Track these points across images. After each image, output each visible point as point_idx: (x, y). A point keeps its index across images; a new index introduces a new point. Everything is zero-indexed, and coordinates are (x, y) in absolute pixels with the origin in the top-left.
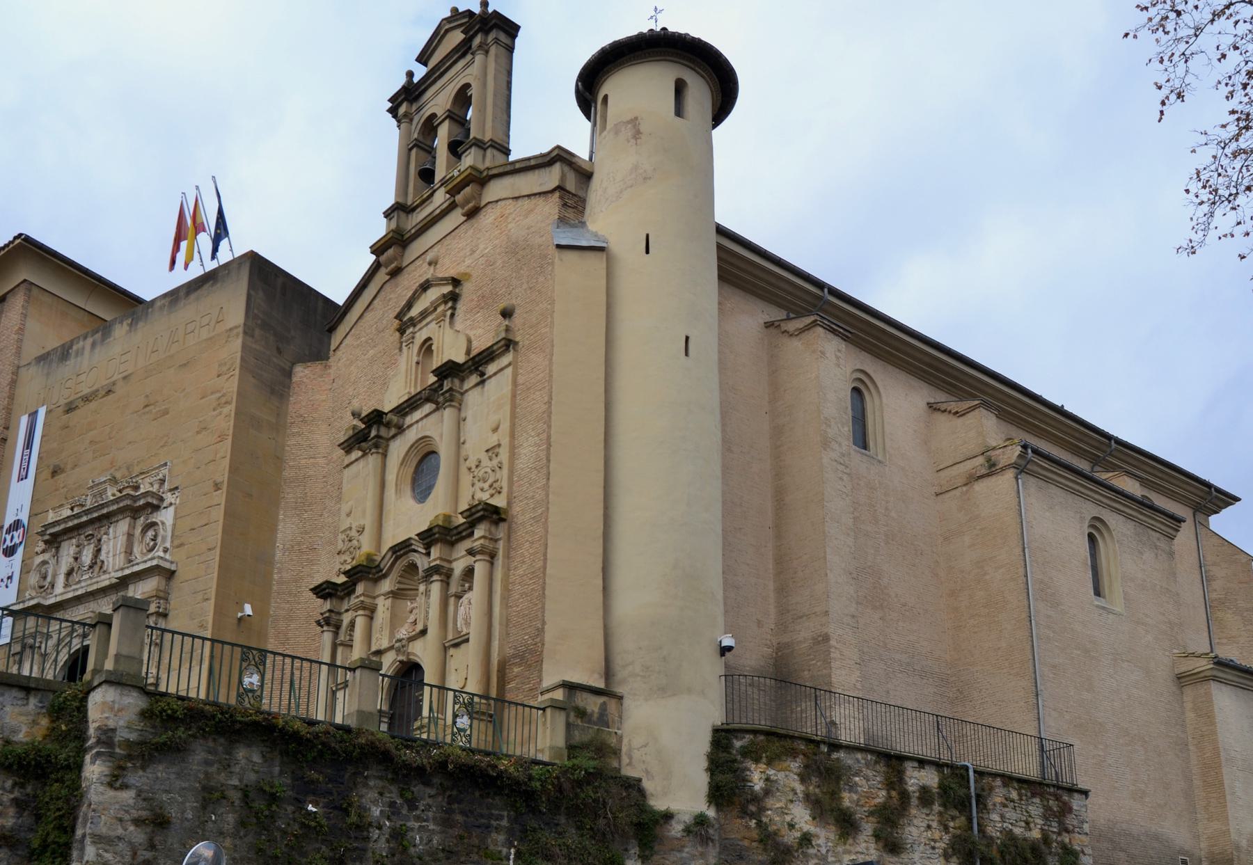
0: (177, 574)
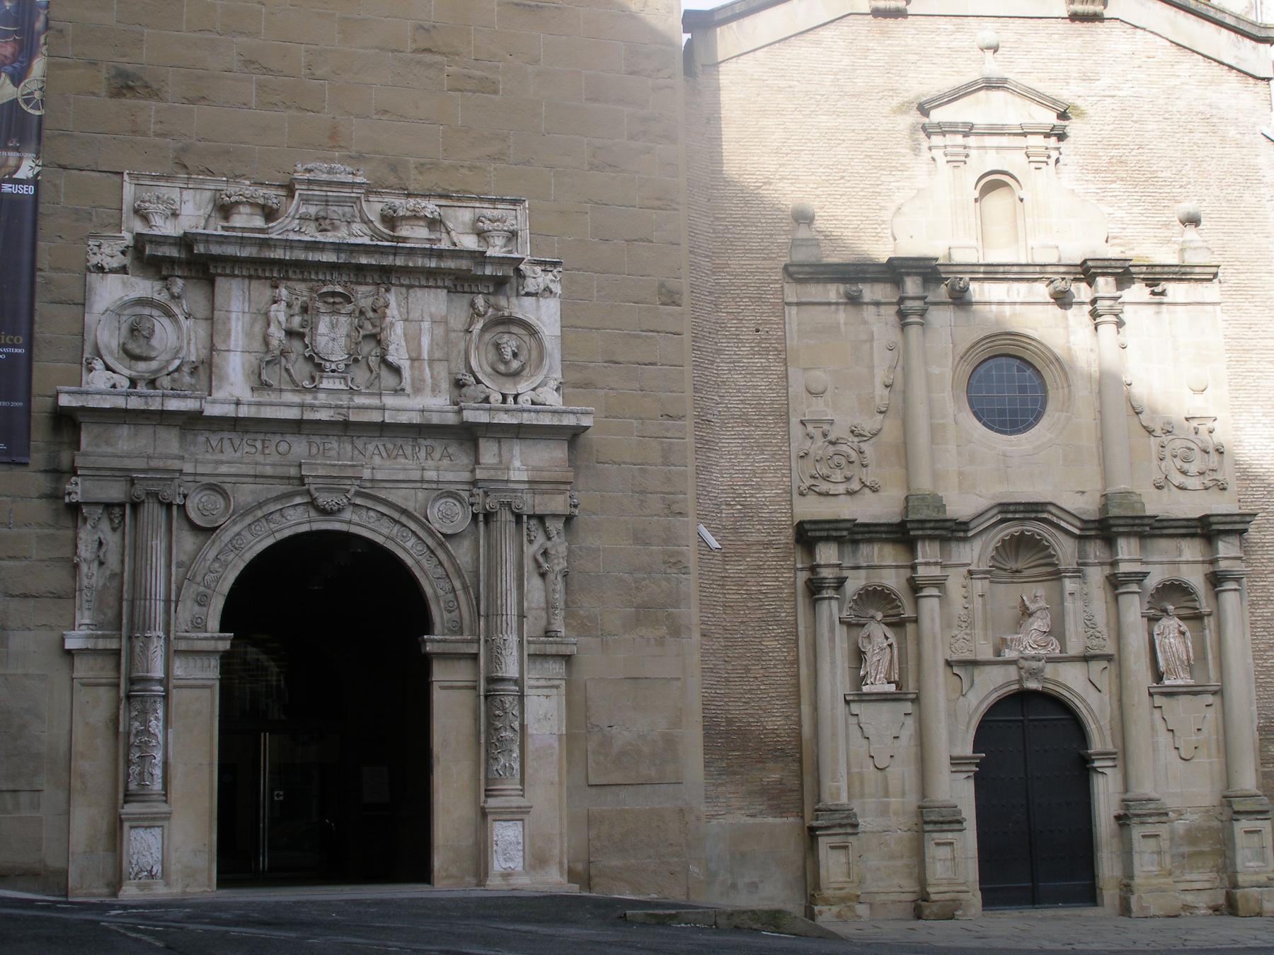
0: (583, 438)
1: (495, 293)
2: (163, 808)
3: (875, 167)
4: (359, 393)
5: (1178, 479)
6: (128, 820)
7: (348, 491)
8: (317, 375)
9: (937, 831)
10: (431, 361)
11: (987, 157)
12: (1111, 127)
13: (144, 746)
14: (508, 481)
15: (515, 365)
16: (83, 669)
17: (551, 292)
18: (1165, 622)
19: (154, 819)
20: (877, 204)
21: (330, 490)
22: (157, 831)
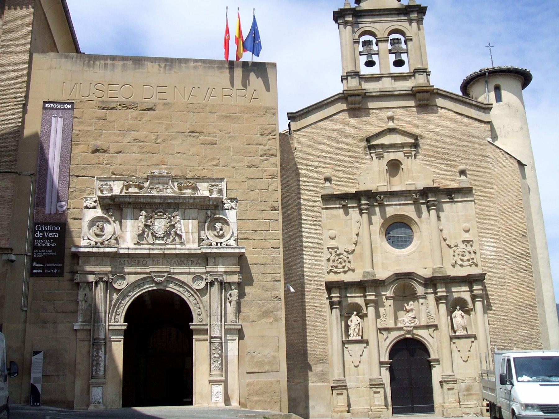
1: (215, 210)
2: (103, 380)
3: (352, 161)
4: (168, 244)
5: (460, 262)
6: (92, 384)
7: (165, 276)
8: (154, 238)
9: (374, 388)
10: (192, 233)
11: (391, 156)
12: (434, 142)
13: (97, 360)
14: (217, 272)
15: (221, 232)
16: (80, 336)
17: (234, 208)
18: (456, 312)
19: (100, 384)
20: (353, 173)
21: (159, 277)
22: (101, 388)
